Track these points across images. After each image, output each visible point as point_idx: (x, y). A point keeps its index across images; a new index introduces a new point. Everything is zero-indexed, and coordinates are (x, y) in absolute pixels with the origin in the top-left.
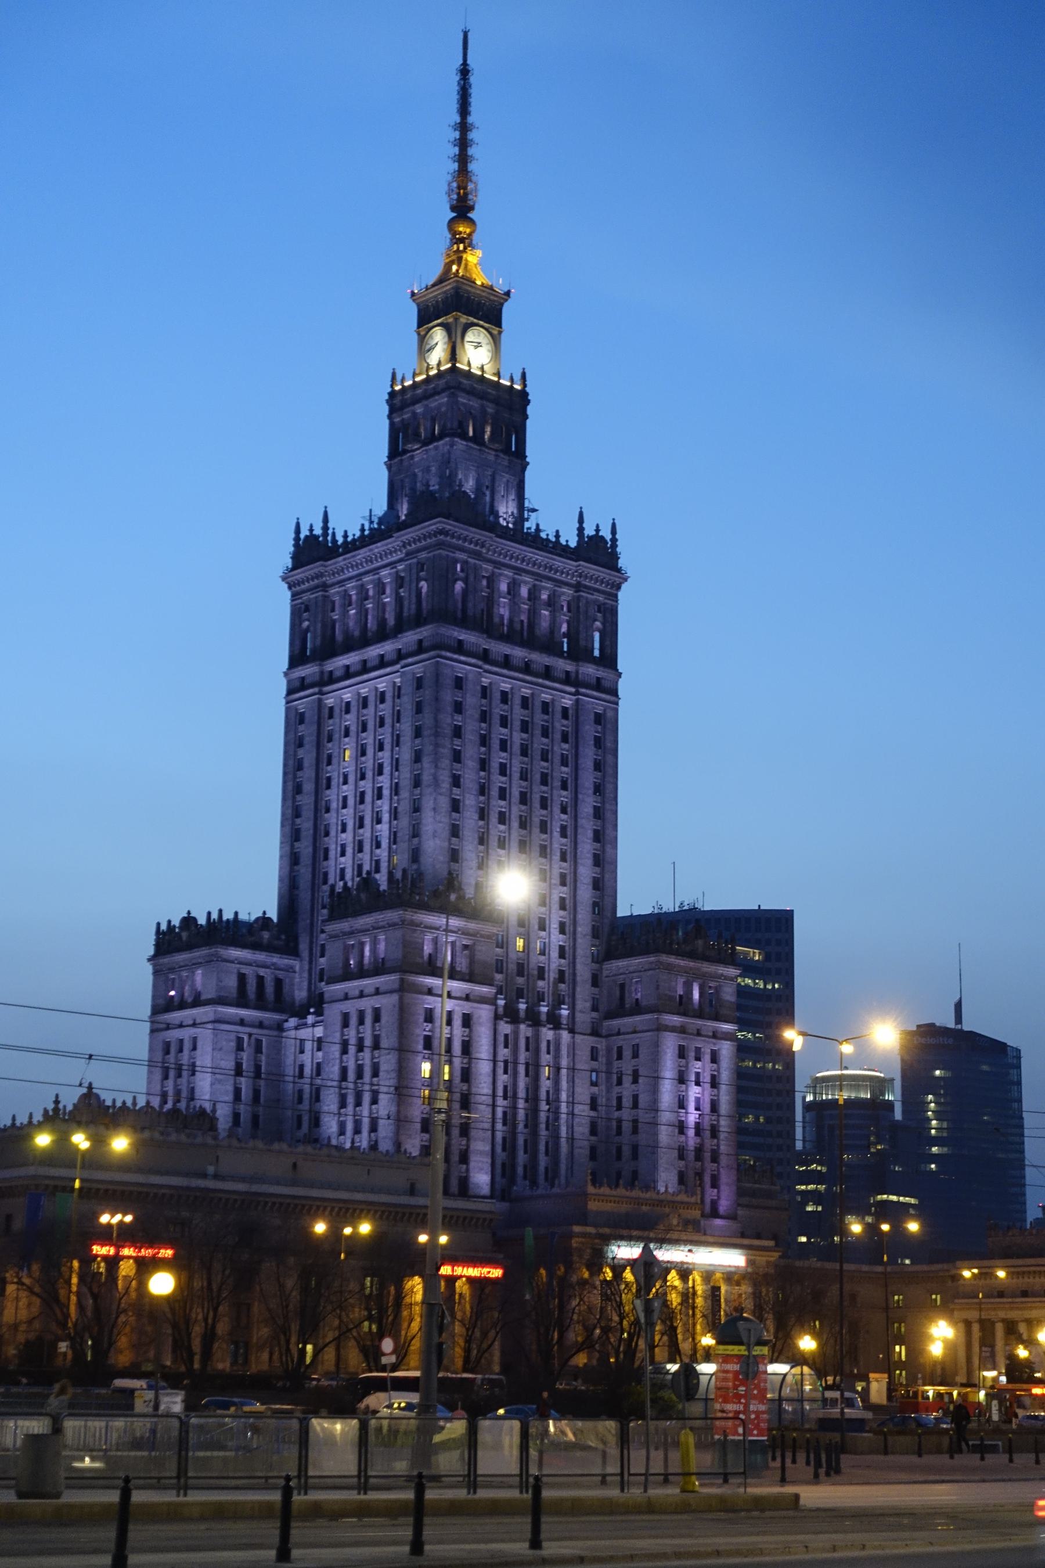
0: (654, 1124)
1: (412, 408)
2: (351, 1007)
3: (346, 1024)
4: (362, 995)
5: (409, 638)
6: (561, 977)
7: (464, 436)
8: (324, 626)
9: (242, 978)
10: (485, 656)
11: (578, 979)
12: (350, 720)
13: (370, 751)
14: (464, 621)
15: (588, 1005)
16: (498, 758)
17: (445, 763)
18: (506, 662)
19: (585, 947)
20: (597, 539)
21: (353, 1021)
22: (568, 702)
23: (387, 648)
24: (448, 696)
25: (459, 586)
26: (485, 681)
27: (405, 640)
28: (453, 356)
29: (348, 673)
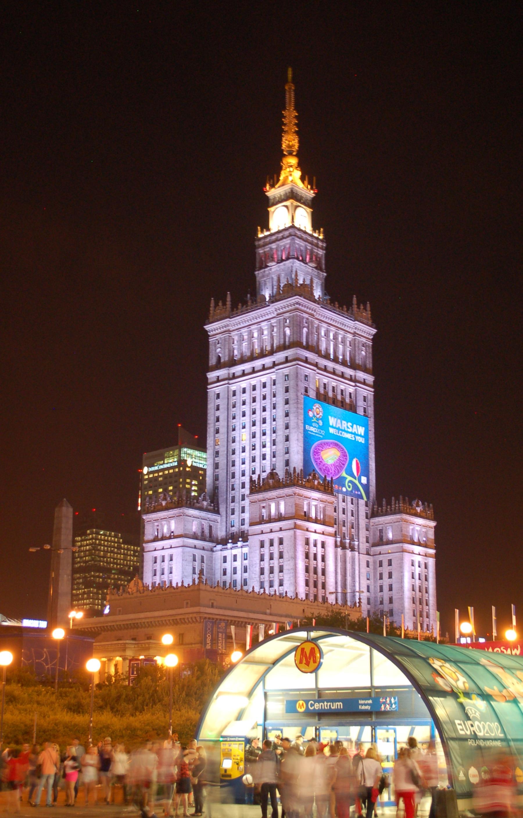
0: (402, 598)
1: (270, 246)
2: (266, 538)
3: (262, 546)
4: (271, 531)
5: (280, 356)
8: (229, 351)
11: (360, 527)
13: (258, 412)
14: (308, 348)
15: (365, 540)
21: (267, 544)
22: (351, 390)
23: (267, 361)
25: (305, 330)
27: (278, 356)
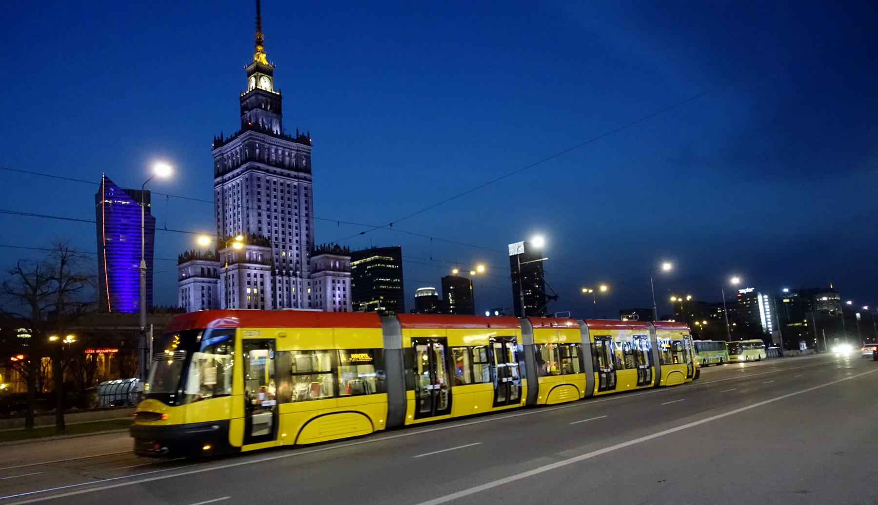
0: (326, 302)
5: (244, 166)
6: (298, 262)
7: (261, 108)
9: (202, 269)
10: (268, 171)
12: (231, 193)
14: (261, 161)
16: (273, 200)
17: (255, 202)
18: (275, 173)
19: (305, 254)
20: (303, 136)
22: (296, 184)
24: (255, 183)
25: (258, 151)
26: (268, 178)
28: (256, 84)
29: (230, 179)
